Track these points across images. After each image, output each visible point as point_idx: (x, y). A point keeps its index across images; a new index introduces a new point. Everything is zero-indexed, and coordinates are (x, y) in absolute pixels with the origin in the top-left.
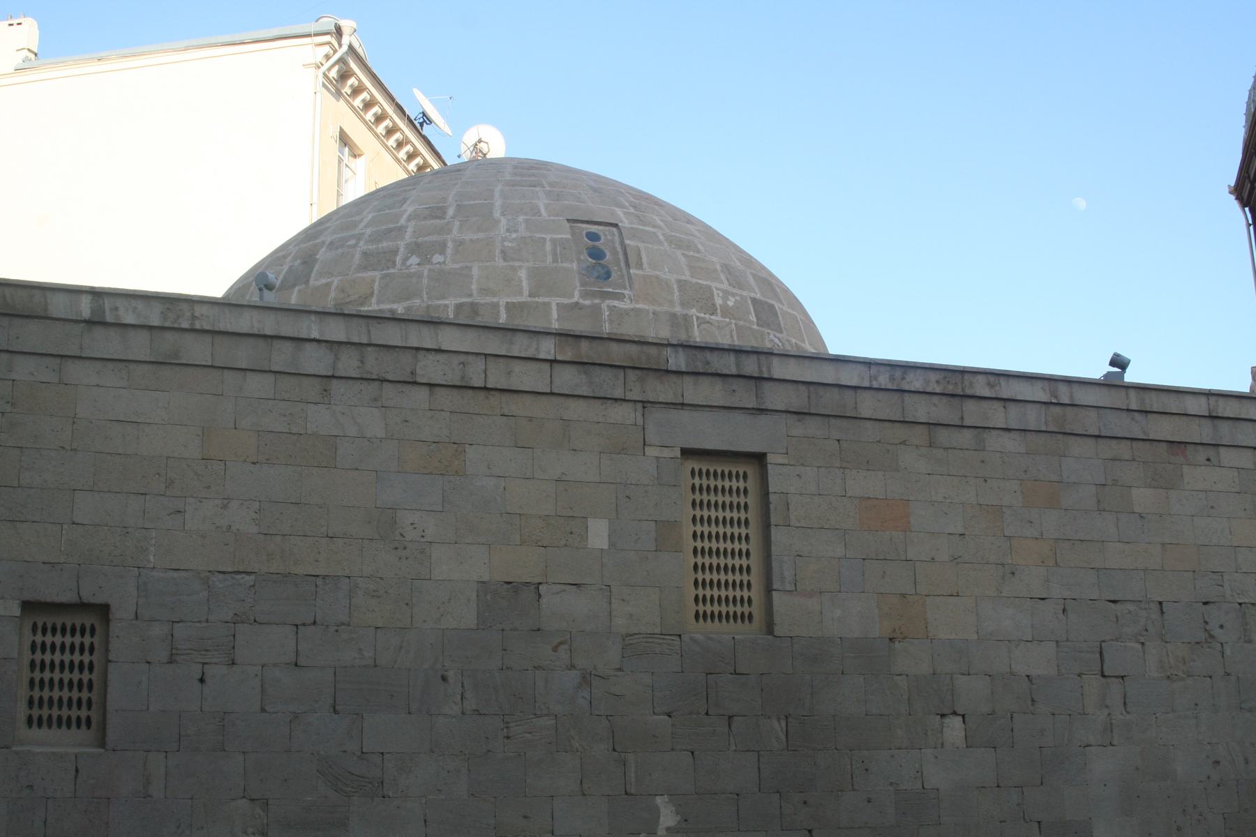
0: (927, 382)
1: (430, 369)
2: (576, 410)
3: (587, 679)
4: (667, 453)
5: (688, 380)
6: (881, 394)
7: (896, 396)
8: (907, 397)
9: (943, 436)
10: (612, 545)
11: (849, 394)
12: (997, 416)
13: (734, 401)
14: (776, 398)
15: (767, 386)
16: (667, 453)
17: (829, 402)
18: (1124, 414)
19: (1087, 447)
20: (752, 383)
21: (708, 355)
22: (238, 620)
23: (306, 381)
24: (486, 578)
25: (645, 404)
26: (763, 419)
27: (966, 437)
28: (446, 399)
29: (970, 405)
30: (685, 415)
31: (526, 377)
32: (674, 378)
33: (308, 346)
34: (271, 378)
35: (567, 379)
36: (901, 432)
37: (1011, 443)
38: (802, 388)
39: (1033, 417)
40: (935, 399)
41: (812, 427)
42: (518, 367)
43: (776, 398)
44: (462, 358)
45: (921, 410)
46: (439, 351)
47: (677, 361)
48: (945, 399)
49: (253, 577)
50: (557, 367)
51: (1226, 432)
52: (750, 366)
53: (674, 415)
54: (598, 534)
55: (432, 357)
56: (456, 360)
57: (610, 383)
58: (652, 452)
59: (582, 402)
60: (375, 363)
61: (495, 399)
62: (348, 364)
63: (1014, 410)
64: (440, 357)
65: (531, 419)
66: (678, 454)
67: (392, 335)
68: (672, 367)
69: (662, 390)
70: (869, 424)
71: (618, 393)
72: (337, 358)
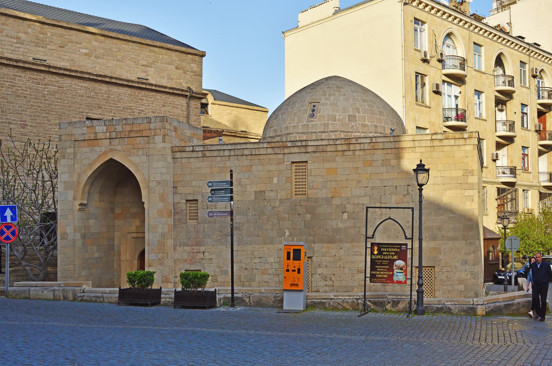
1: (246, 152)
2: (272, 157)
3: (273, 207)
4: (288, 163)
5: (292, 148)
6: (332, 145)
7: (335, 146)
8: (337, 146)
9: (346, 153)
10: (278, 182)
11: (325, 147)
12: (358, 147)
13: (301, 151)
14: (310, 149)
15: (307, 147)
16: (288, 163)
17: (320, 148)
18: (390, 143)
19: (380, 152)
20: (305, 147)
21: (295, 142)
23: (226, 157)
24: (256, 190)
25: (284, 154)
26: (307, 154)
27: (350, 153)
28: (249, 157)
29: (352, 146)
30: (291, 155)
31: (262, 151)
32: (289, 148)
33: (226, 151)
34: (220, 157)
35: (270, 151)
36: (336, 153)
37: (361, 153)
38: (315, 146)
39: (366, 146)
40: (344, 145)
41: (317, 154)
42: (261, 150)
43: (310, 149)
44: (251, 149)
45: (340, 148)
46: (247, 148)
47: (289, 144)
48: (346, 145)
50: (268, 149)
51: (417, 144)
52: (304, 144)
53: (290, 155)
54: (275, 181)
55: (246, 150)
56: (250, 149)
57: (277, 151)
58: (285, 163)
59: (272, 155)
60: (237, 152)
61: (257, 156)
62: (232, 153)
63: (362, 145)
64: (247, 150)
65: (263, 159)
66: (290, 163)
67: (239, 147)
68: (288, 146)
69: (286, 151)
70: (329, 152)
71: (279, 152)
72: (230, 152)
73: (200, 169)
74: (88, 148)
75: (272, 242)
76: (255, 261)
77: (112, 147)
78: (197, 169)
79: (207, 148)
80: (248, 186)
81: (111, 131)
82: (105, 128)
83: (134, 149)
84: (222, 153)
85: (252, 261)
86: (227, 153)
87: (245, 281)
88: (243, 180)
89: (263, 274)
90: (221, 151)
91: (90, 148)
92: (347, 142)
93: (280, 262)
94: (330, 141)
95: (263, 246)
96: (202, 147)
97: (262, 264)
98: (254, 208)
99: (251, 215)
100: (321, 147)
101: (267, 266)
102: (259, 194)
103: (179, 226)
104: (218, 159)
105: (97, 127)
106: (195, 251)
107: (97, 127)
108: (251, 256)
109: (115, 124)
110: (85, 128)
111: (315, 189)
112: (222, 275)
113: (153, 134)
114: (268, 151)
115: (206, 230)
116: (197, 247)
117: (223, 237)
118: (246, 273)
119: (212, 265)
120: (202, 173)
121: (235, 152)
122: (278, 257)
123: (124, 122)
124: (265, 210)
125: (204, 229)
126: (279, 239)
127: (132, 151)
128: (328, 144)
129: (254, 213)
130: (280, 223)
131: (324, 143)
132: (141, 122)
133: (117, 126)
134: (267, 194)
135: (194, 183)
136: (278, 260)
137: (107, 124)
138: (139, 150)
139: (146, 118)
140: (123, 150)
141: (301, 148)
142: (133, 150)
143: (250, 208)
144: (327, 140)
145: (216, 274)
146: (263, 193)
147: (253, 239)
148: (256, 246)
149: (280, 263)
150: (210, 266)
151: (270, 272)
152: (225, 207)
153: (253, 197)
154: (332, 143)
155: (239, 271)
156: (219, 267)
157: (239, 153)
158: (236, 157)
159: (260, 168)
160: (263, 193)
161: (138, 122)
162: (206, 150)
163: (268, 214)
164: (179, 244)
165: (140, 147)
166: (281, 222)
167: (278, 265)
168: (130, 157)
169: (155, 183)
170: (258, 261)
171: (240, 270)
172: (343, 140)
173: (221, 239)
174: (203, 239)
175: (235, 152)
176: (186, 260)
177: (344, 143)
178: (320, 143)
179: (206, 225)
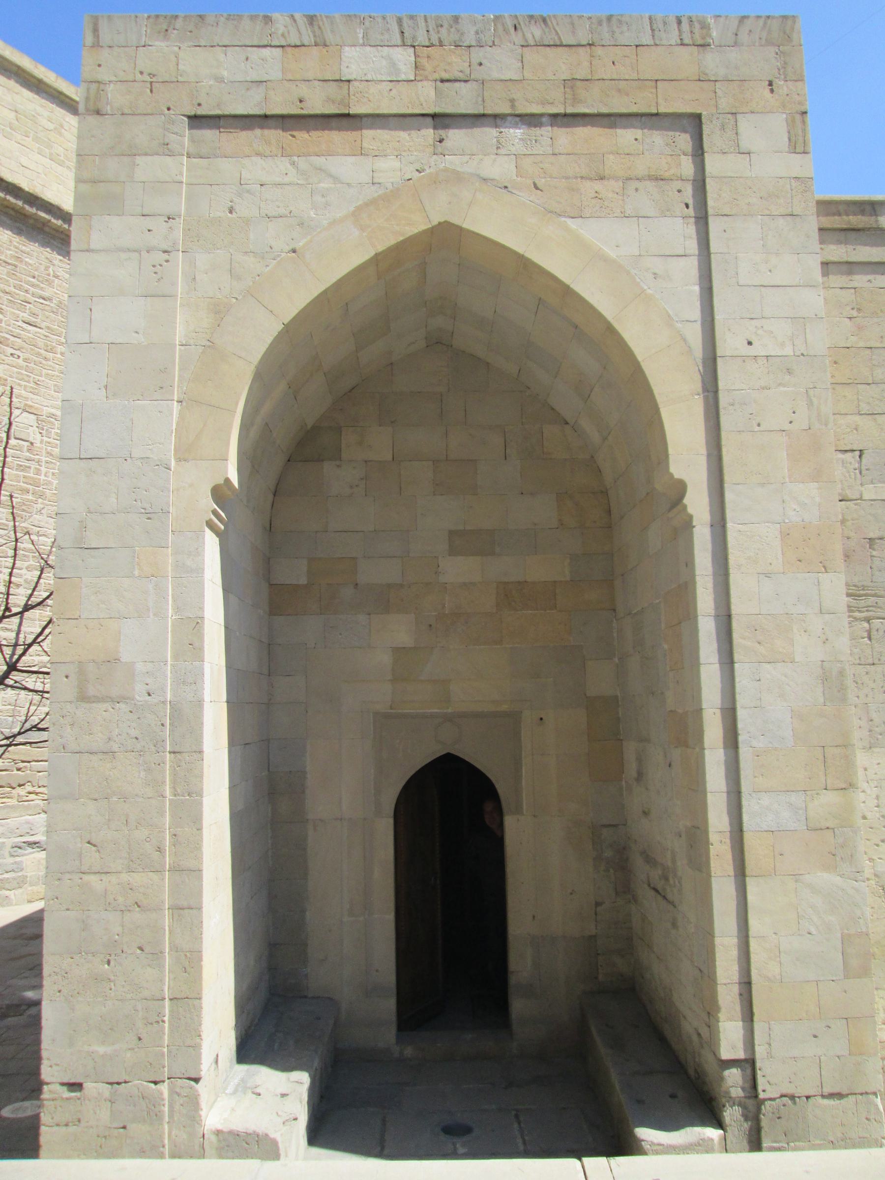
74: (283, 164)
77: (452, 161)
81: (446, 76)
82: (404, 58)
83: (602, 178)
91: (302, 163)
105: (348, 52)
107: (348, 52)
109: (470, 39)
110: (266, 52)
113: (724, 104)
123: (535, 32)
127: (590, 188)
132: (647, 39)
133: (477, 55)
137: (422, 38)
138: (635, 184)
139: (679, 22)
140: (529, 182)
142: (598, 186)
161: (627, 37)
165: (641, 171)
168: (572, 224)
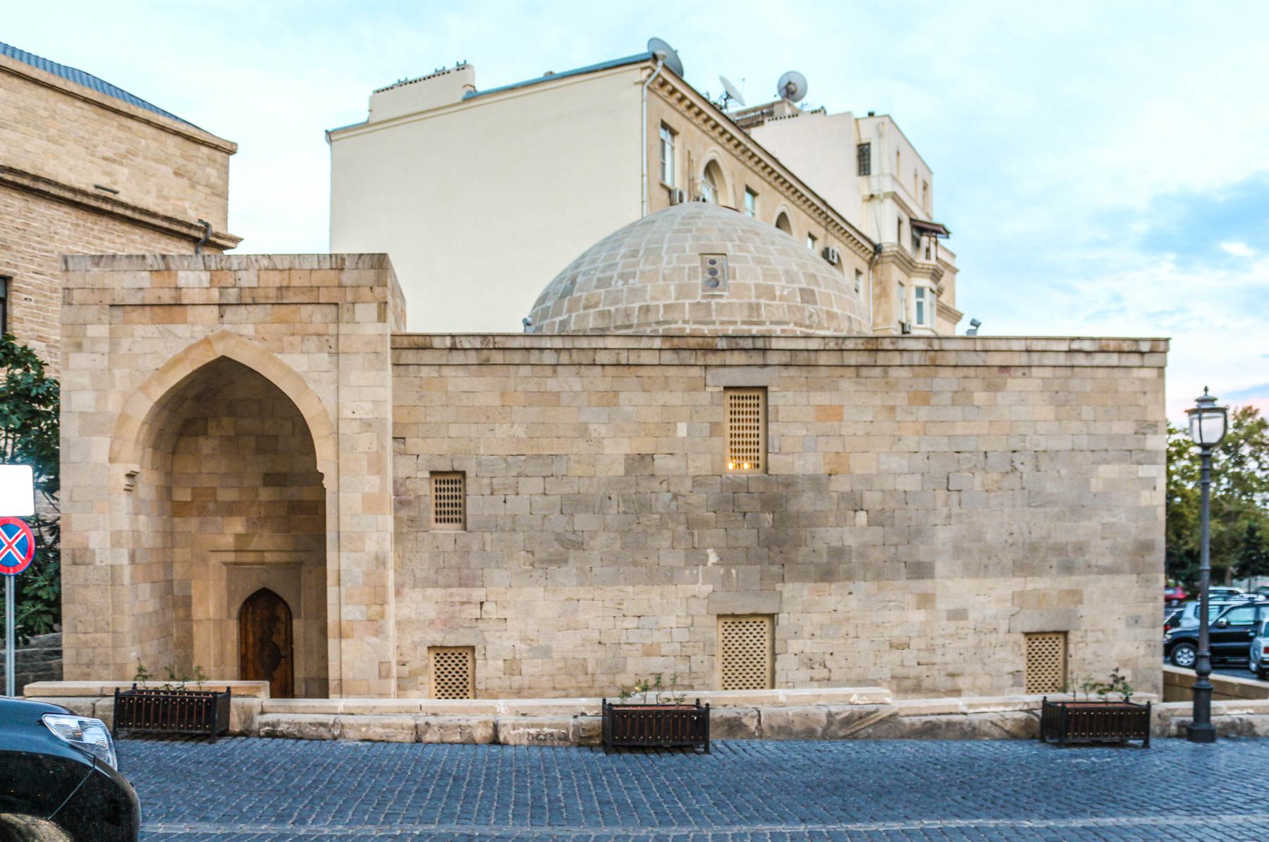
0: (857, 344)
4: (717, 389)
7: (838, 353)
8: (845, 353)
10: (689, 434)
11: (812, 355)
14: (773, 358)
16: (717, 389)
17: (802, 358)
22: (519, 475)
25: (706, 366)
26: (767, 370)
30: (726, 370)
31: (647, 358)
32: (721, 353)
35: (667, 357)
42: (643, 353)
45: (852, 359)
49: (524, 458)
53: (721, 370)
54: (682, 430)
57: (688, 357)
58: (709, 389)
61: (633, 369)
65: (650, 377)
66: (722, 389)
69: (713, 359)
71: (692, 362)
73: (470, 395)
75: (670, 576)
76: (626, 625)
78: (465, 394)
79: (495, 343)
80: (606, 442)
84: (534, 357)
85: (618, 624)
86: (549, 358)
87: (599, 671)
88: (592, 427)
89: (647, 654)
90: (532, 351)
92: (869, 347)
93: (692, 625)
94: (827, 340)
95: (647, 587)
96: (479, 339)
97: (645, 632)
98: (623, 496)
99: (615, 511)
100: (806, 354)
101: (657, 637)
102: (639, 461)
103: (412, 536)
104: (524, 371)
106: (457, 599)
108: (614, 612)
111: (788, 454)
112: (534, 658)
114: (662, 359)
115: (488, 548)
116: (463, 591)
117: (536, 566)
118: (601, 653)
119: (505, 635)
120: (477, 404)
121: (571, 356)
122: (688, 615)
124: (654, 499)
125: (484, 544)
126: (692, 573)
128: (822, 348)
129: (622, 509)
130: (692, 534)
131: (813, 345)
134: (659, 461)
135: (454, 430)
136: (689, 621)
141: (752, 353)
143: (613, 496)
144: (820, 340)
145: (518, 657)
146: (648, 459)
147: (621, 571)
148: (630, 589)
149: (692, 629)
150: (500, 637)
151: (664, 650)
152: (542, 491)
153: (621, 471)
154: (832, 345)
155: (581, 649)
156: (524, 639)
157: (585, 358)
158: (575, 369)
159: (640, 398)
160: (648, 459)
162: (491, 346)
163: (661, 510)
164: (411, 582)
166: (696, 532)
167: (687, 633)
169: (355, 425)
170: (635, 625)
171: (583, 645)
172: (860, 341)
173: (531, 570)
174: (480, 572)
175: (571, 356)
176: (432, 623)
177: (862, 347)
178: (801, 344)
179: (488, 536)
